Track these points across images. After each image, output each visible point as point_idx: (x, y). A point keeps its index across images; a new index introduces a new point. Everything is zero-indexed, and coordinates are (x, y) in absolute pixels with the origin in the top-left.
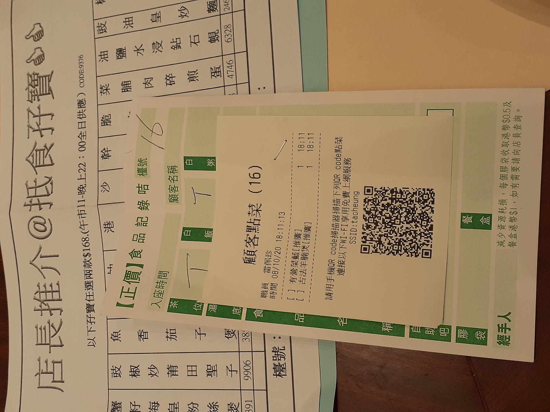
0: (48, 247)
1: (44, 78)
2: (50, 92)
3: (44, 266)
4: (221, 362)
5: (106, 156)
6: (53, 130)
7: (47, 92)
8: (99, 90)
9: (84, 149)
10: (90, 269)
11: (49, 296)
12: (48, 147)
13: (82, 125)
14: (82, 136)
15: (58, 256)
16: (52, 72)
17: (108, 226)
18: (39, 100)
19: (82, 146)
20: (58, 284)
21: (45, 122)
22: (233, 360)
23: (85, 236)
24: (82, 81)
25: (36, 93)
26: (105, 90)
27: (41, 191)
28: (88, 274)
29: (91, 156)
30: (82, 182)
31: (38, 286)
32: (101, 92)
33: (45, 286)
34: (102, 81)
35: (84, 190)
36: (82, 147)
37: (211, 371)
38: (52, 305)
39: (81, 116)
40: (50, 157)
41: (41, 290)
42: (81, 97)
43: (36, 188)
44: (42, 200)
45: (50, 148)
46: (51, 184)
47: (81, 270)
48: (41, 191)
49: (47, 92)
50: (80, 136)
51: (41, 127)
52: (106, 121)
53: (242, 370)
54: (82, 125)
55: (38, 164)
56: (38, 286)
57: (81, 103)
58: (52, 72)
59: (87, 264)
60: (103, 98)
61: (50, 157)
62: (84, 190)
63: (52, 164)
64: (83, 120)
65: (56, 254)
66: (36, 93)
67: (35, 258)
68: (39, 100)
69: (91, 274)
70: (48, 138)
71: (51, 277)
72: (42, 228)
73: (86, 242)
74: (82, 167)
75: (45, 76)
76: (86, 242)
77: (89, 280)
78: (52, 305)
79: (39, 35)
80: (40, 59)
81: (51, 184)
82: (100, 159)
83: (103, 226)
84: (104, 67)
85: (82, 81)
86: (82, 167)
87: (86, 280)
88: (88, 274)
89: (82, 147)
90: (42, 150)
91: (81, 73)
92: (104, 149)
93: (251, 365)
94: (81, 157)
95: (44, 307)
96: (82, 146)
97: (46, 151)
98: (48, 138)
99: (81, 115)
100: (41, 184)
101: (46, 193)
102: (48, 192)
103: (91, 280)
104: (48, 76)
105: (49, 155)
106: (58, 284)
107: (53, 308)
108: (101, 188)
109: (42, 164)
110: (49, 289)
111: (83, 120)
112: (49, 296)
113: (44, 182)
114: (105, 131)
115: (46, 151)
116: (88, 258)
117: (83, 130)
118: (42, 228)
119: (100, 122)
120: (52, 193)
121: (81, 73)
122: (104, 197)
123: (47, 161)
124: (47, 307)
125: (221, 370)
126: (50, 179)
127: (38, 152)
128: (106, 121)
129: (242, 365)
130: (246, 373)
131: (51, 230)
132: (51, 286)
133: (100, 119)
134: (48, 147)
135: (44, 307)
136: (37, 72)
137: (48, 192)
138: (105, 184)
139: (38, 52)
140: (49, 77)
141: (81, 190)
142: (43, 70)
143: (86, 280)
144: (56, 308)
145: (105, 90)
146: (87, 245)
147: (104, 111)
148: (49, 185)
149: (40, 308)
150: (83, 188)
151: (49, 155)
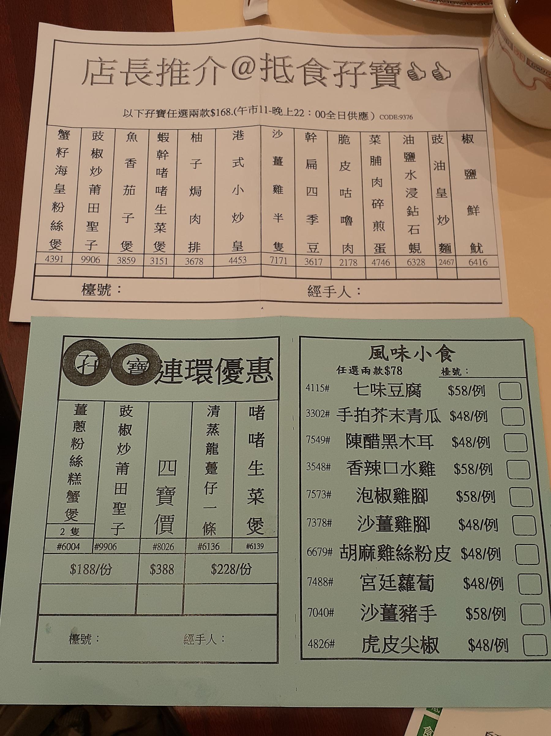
0: (224, 75)
1: (393, 80)
2: (379, 85)
3: (206, 70)
4: (100, 236)
5: (308, 137)
6: (340, 87)
7: (379, 83)
8: (375, 134)
9: (318, 116)
10: (199, 115)
11: (176, 74)
12: (323, 81)
13: (342, 115)
14: (331, 115)
15: (214, 84)
16: (398, 88)
17: (239, 135)
18: (372, 74)
19: (320, 114)
20: (187, 83)
21: (349, 79)
22: (101, 247)
23: (232, 112)
24: (386, 117)
25: (379, 71)
26: (375, 139)
27: (280, 71)
28: (194, 114)
29: (311, 122)
30: (285, 112)
31: (187, 64)
32: (373, 136)
33: (186, 70)
34: (384, 138)
35: (276, 113)
36: (320, 114)
37: (92, 226)
38: (167, 76)
39: (351, 115)
40: (313, 82)
41: (182, 66)
42: (370, 116)
43: (284, 66)
44: (271, 72)
45: (322, 83)
46: (286, 82)
47: (199, 107)
48: (280, 71)
49: (379, 83)
50: (331, 113)
51: (344, 75)
52: (343, 139)
53: (91, 255)
54: (342, 115)
55: (307, 70)
56: (187, 64)
57: (364, 115)
58: (398, 88)
59: (204, 113)
60: (366, 138)
61: (313, 82)
62: (276, 113)
63: (305, 84)
64: (347, 117)
65: (216, 83)
66: (379, 71)
67: (214, 62)
68: (372, 74)
69: (194, 115)
70: (332, 81)
71: (194, 77)
72: (243, 70)
73: (226, 112)
74: (299, 113)
75: (395, 81)
76: (226, 112)
77: (189, 113)
78: (167, 76)
79: (438, 76)
80: (413, 76)
81: (286, 82)
82: (306, 131)
83: (239, 129)
84: (397, 139)
85: (386, 117)
86: (299, 113)
87: (189, 111)
88: (194, 114)
89: (320, 114)
90: (321, 74)
91: (395, 117)
92: (315, 136)
93: (95, 263)
94: (310, 113)
95: (166, 68)
96: (320, 114)
97: (319, 78)
98: (332, 81)
99: (352, 115)
100: (287, 71)
101: (277, 76)
102: (278, 77)
103: (189, 116)
104: (395, 84)
105: (315, 82)
106: (187, 83)
107: (164, 77)
108: (277, 129)
109: (307, 73)
110: (183, 74)
111: (347, 117)
112: (176, 74)
113: (288, 75)
114: (334, 138)
115: (319, 78)
116: (210, 113)
117: (336, 116)
118: (243, 70)
119: (343, 134)
120: (277, 82)
121: (395, 117)
122: (268, 133)
123: (309, 79)
124: (165, 71)
125: (92, 236)
126: (291, 81)
127: (319, 71)
128: (343, 139)
129: (96, 255)
130: (88, 258)
131: (240, 79)
132: (186, 76)
133: (346, 134)
134: (323, 81)
135: (166, 68)
136: (400, 73)
137: (278, 77)
138: (280, 134)
139: (420, 74)
140: (394, 85)
141: (277, 110)
142: (402, 79)
143: (189, 111)
144: (164, 80)
145: (375, 139)
146: (223, 113)
147: (354, 138)
148: (284, 79)
149: (165, 64)
150: (279, 112)
151: (315, 82)
